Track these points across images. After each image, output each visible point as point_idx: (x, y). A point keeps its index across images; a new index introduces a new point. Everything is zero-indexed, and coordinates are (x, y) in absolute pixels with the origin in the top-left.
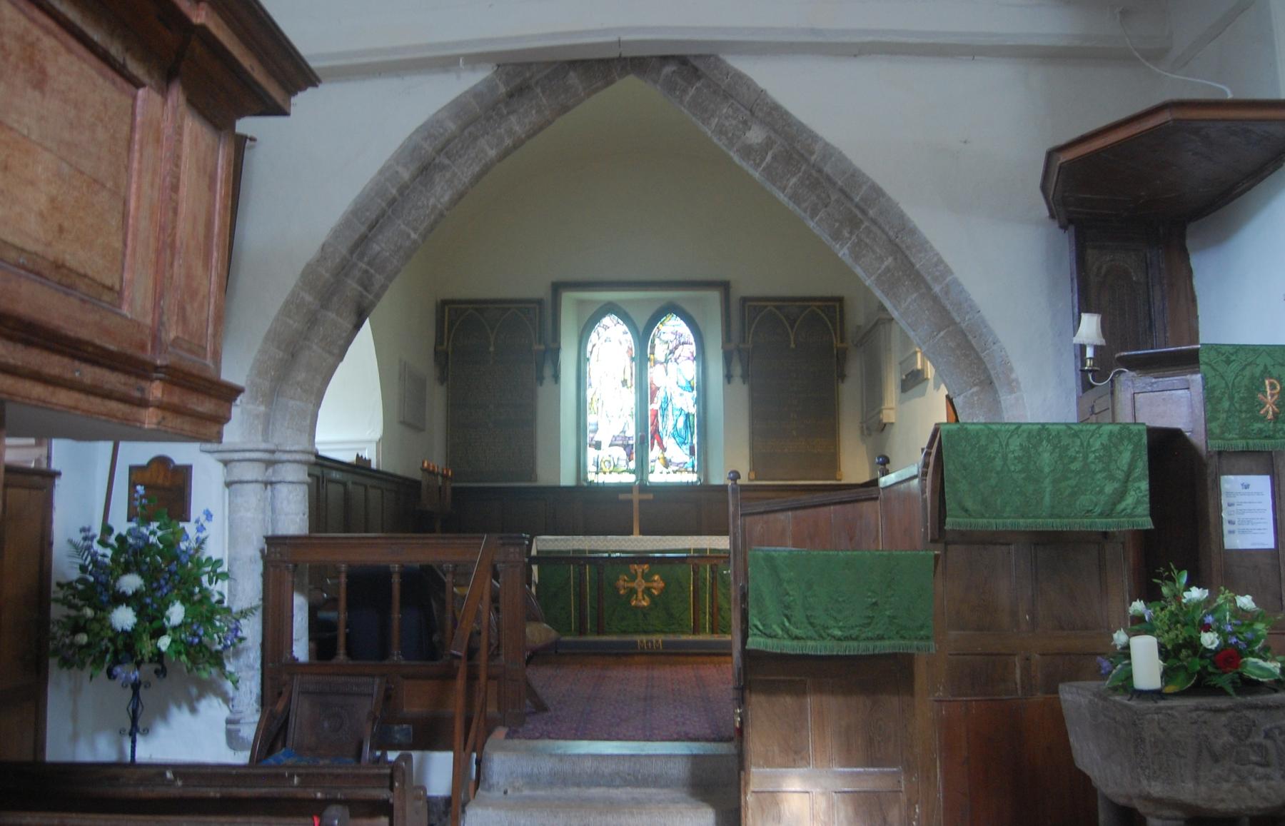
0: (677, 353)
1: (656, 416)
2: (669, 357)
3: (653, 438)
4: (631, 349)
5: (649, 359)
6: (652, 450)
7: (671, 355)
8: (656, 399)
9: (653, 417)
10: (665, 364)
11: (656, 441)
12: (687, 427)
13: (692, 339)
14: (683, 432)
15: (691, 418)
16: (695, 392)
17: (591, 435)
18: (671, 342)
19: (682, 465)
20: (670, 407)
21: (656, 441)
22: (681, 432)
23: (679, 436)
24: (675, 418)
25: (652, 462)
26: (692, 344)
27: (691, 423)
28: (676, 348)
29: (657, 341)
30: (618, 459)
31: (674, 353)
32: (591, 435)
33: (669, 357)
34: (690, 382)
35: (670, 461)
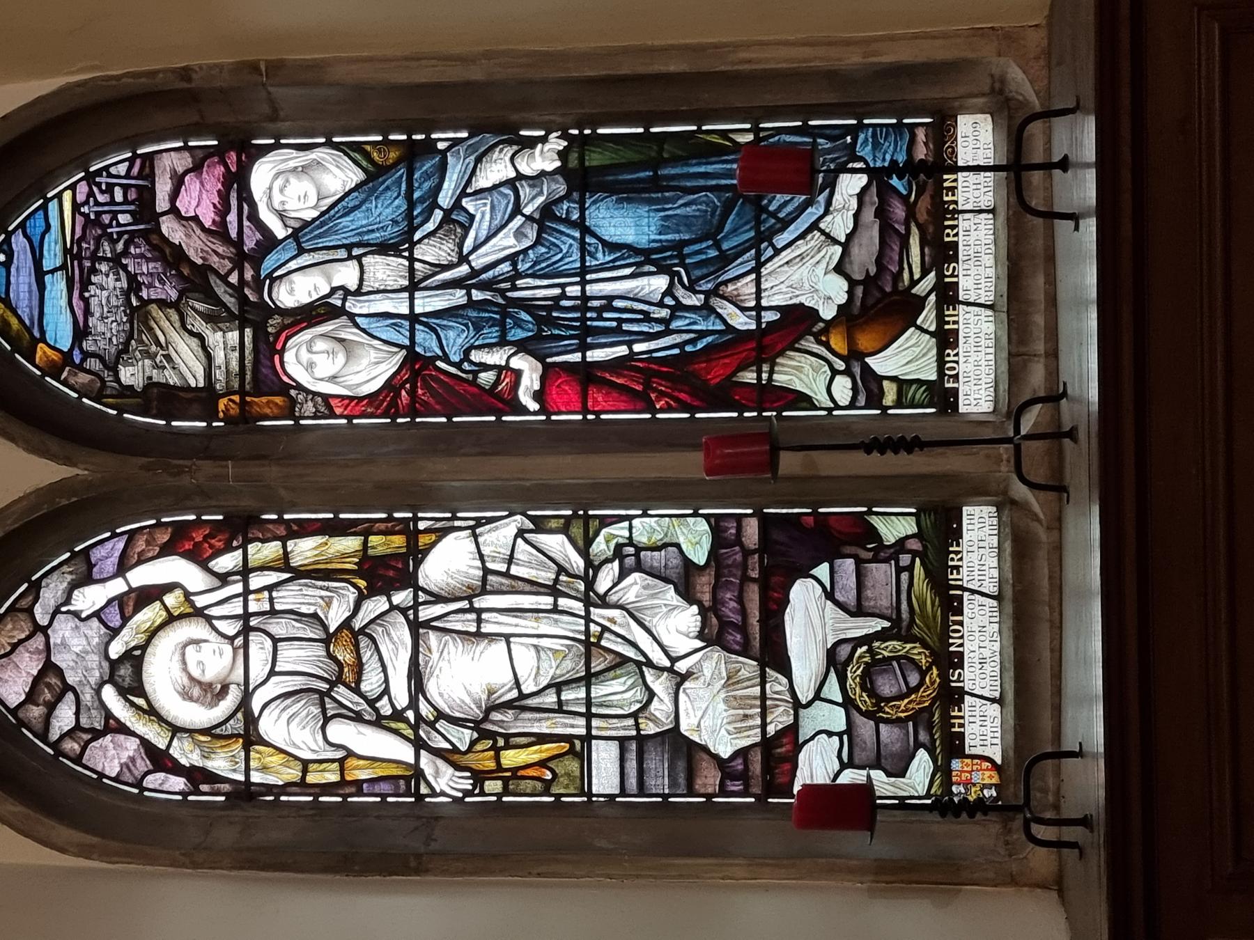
0: (195, 246)
1: (587, 374)
2: (230, 301)
3: (725, 395)
4: (181, 530)
5: (245, 419)
6: (803, 400)
7: (220, 290)
8: (486, 378)
9: (597, 396)
10: (274, 323)
11: (749, 377)
12: (656, 184)
13: (117, 162)
14: (682, 208)
15: (595, 159)
16: (442, 138)
17: (709, 779)
18: (134, 285)
19: (899, 211)
20: (539, 290)
21: (749, 377)
22: (686, 222)
23: (712, 234)
24: (602, 257)
25: (875, 399)
26: (150, 158)
27: (630, 155)
28: (173, 257)
29: (130, 375)
30: (858, 611)
31: (206, 269)
32: (709, 779)
33: (230, 301)
34: (374, 176)
35: (869, 282)
